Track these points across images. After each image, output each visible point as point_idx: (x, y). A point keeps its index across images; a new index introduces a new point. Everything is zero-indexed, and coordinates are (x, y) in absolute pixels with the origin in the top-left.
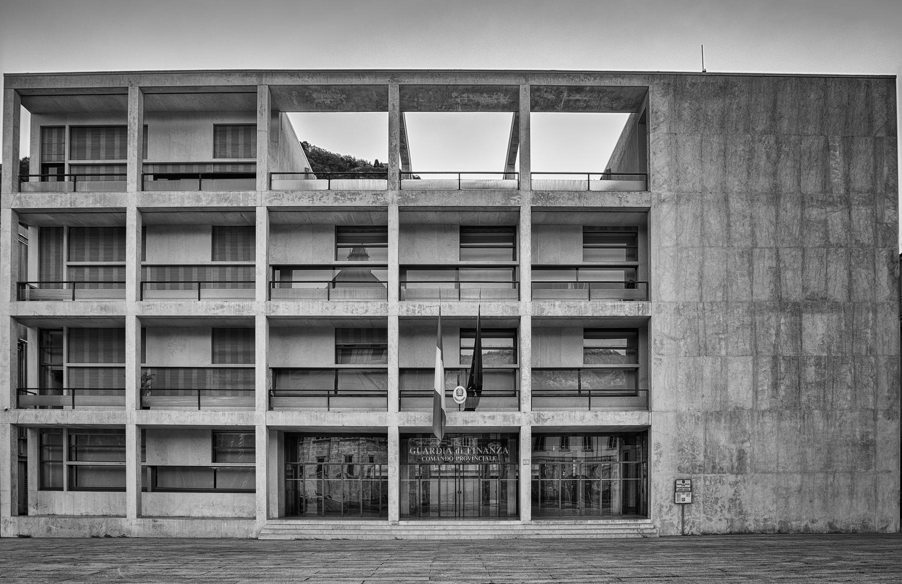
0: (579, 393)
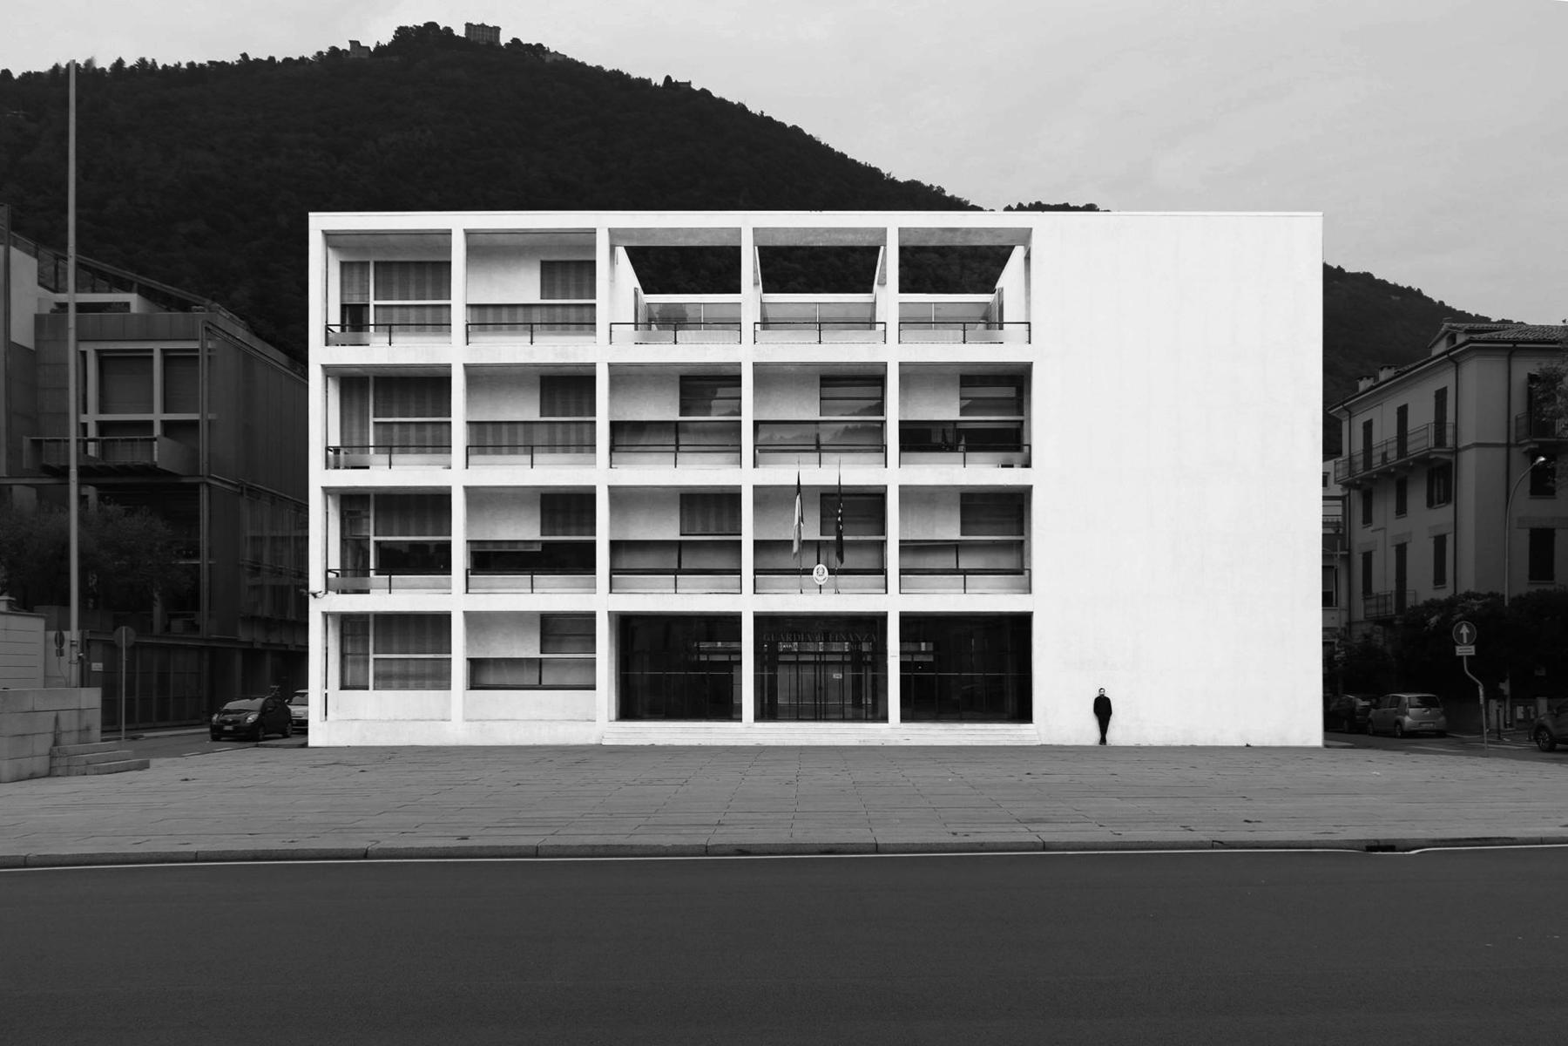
0: (956, 572)
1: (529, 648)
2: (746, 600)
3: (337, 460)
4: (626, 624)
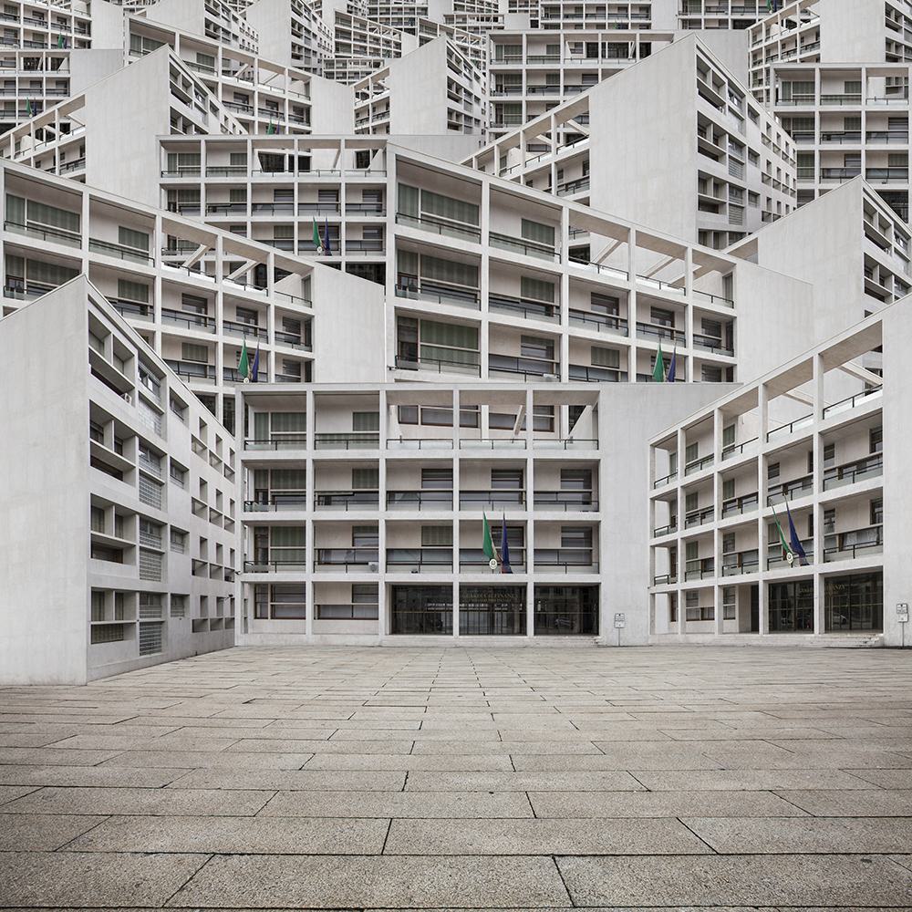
2: (455, 576)
4: (395, 589)
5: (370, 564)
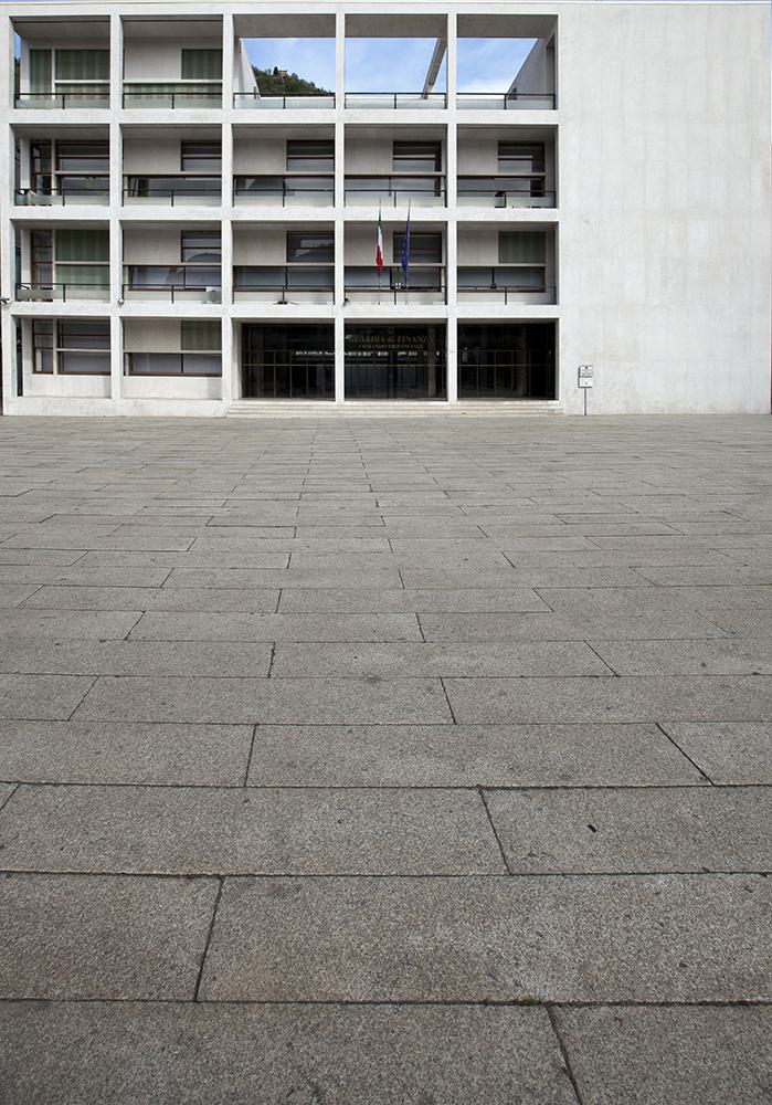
1: (174, 347)
3: (26, 199)
4: (249, 331)
5: (209, 289)
